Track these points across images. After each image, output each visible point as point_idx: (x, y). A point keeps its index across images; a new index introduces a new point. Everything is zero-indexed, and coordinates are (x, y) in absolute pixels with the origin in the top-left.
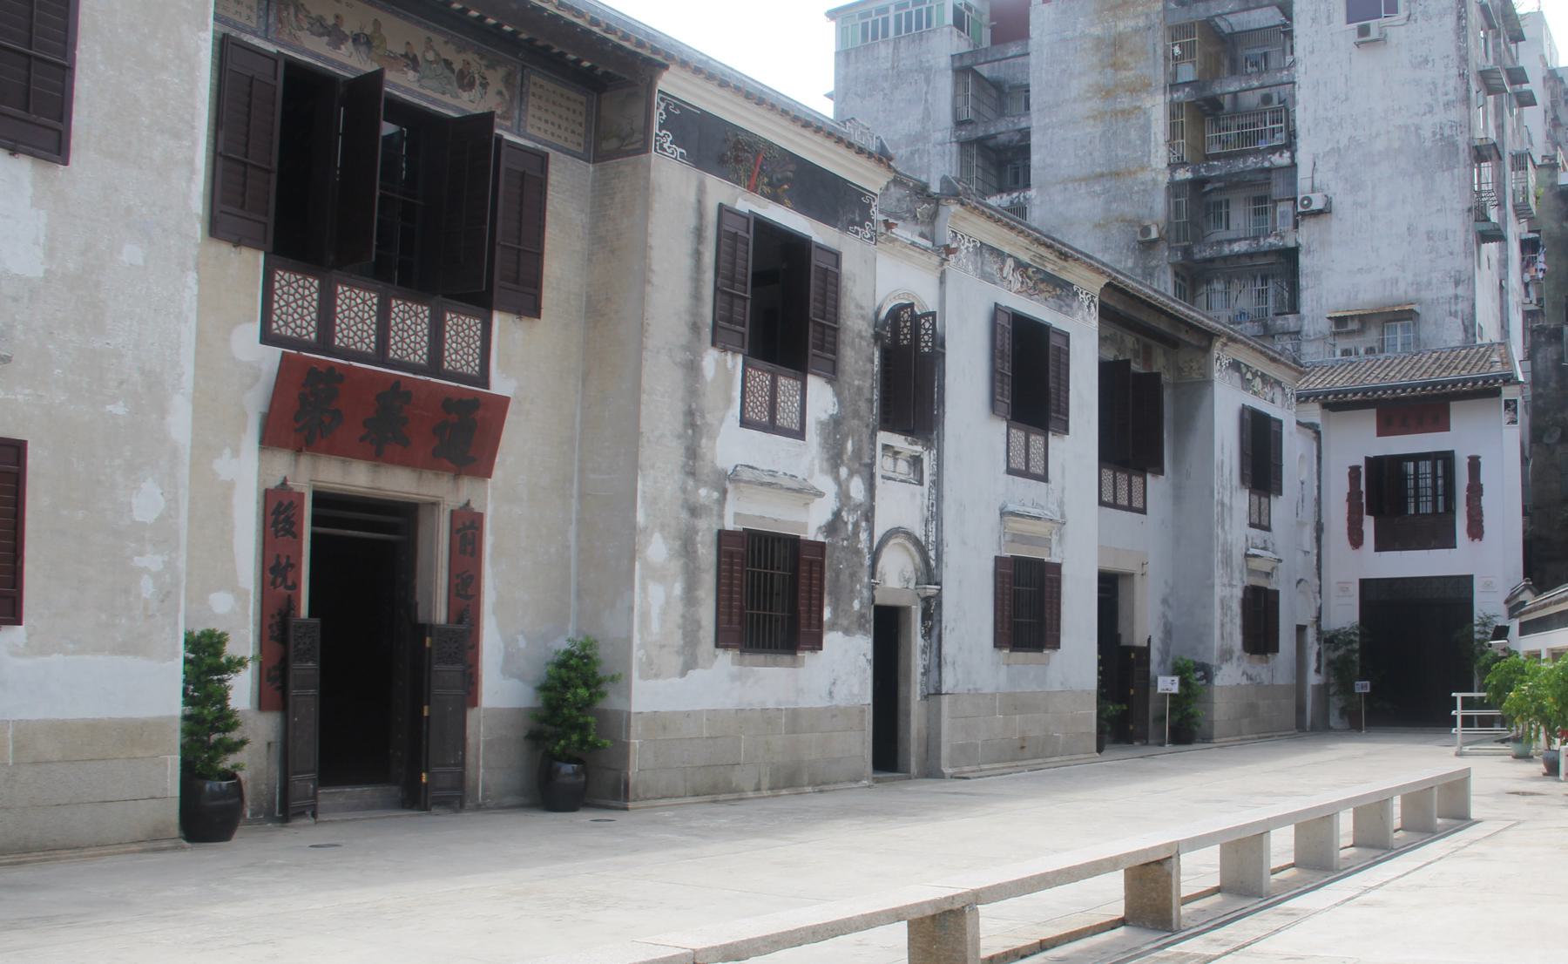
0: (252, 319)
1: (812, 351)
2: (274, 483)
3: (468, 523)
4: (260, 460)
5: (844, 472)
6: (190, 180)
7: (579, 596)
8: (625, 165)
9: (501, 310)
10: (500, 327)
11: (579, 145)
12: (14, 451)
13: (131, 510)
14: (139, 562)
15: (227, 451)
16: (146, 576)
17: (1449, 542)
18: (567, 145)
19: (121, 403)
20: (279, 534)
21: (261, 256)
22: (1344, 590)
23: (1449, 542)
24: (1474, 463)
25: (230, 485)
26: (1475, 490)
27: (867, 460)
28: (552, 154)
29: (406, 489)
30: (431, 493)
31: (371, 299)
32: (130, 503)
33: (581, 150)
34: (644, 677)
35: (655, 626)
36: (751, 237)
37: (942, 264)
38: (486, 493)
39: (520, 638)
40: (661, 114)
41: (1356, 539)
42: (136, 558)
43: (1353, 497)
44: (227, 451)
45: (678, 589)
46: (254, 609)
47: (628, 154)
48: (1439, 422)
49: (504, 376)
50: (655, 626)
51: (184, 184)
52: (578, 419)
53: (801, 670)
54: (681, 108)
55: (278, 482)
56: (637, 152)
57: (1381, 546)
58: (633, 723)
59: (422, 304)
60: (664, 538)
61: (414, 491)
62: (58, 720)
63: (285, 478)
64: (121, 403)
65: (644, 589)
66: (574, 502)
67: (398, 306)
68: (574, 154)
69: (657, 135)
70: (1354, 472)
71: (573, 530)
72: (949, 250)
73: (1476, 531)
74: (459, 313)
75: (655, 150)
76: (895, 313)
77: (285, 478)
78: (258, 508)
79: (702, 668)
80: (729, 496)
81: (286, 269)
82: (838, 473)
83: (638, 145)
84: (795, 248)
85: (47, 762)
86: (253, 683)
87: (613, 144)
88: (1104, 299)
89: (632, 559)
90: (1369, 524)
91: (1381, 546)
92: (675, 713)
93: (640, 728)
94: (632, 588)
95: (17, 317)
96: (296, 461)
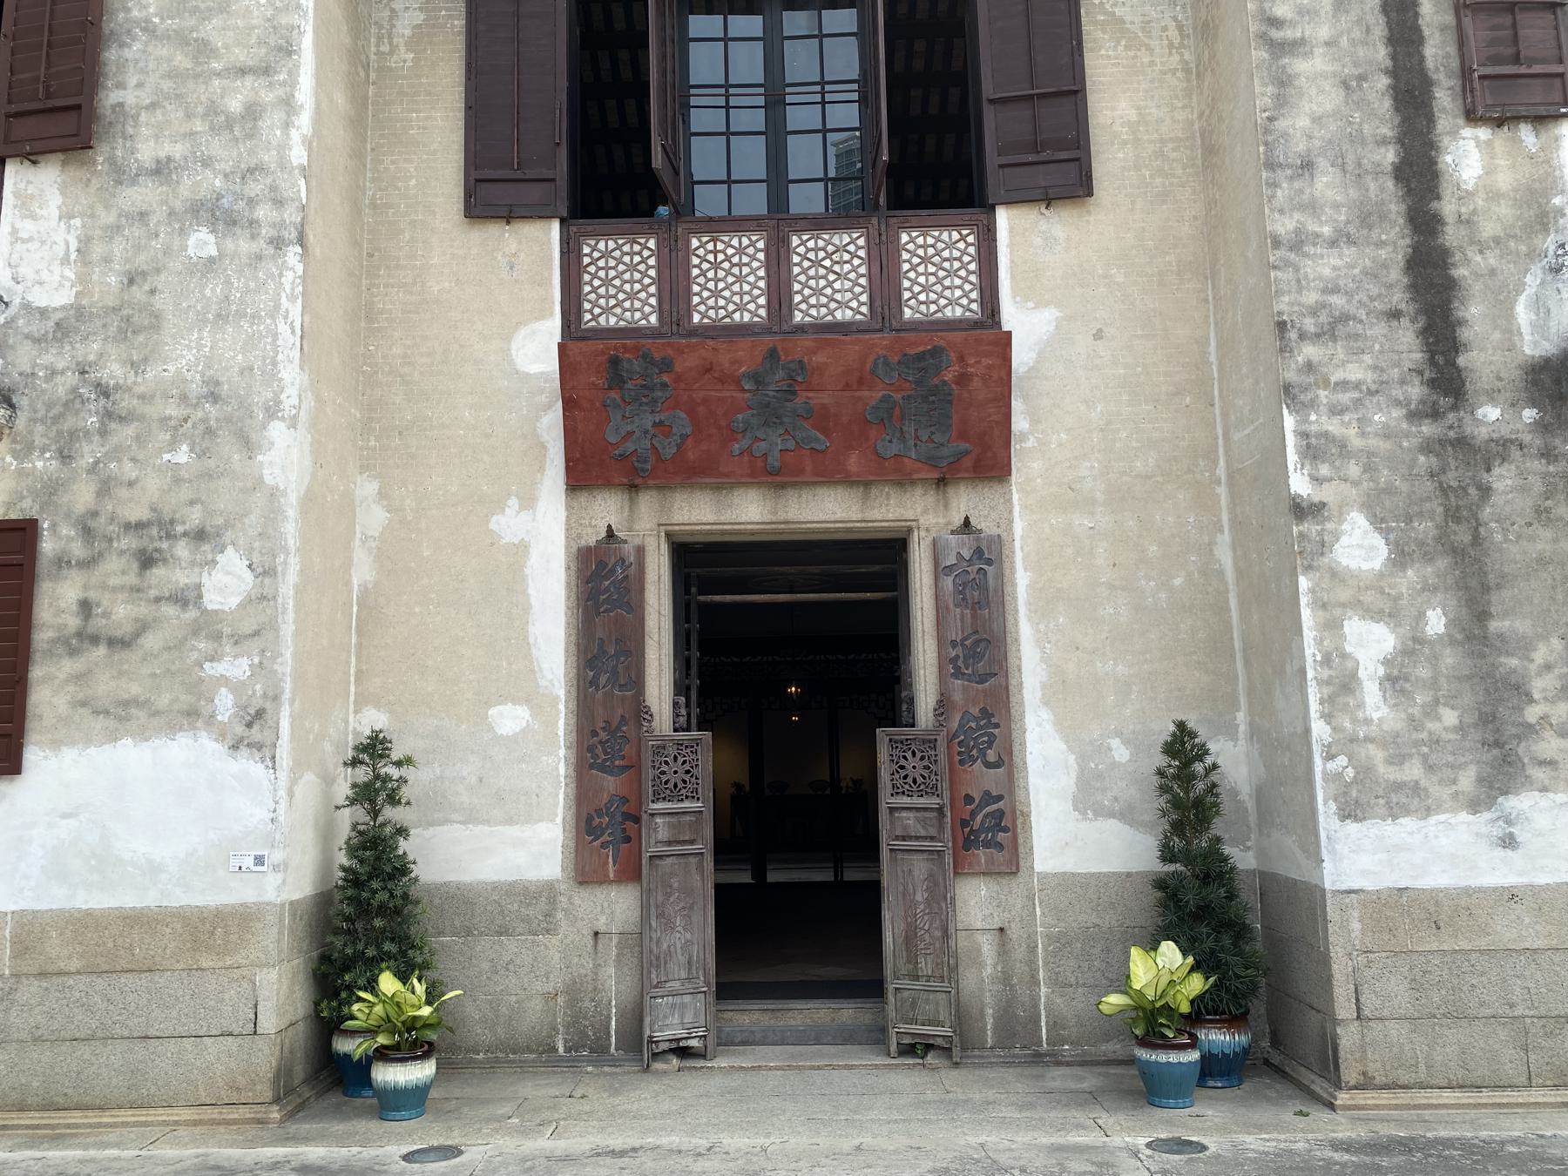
0: (543, 314)
2: (594, 535)
3: (966, 554)
4: (569, 507)
6: (287, 125)
9: (1008, 203)
10: (1011, 230)
12: (23, 533)
13: (200, 596)
14: (211, 669)
15: (513, 502)
16: (223, 690)
19: (185, 448)
20: (602, 610)
21: (555, 227)
25: (522, 549)
29: (840, 514)
30: (891, 516)
31: (753, 244)
32: (199, 586)
34: (1351, 811)
35: (1374, 703)
38: (1010, 500)
39: (1115, 743)
42: (207, 665)
44: (513, 502)
45: (1436, 623)
46: (566, 724)
49: (1031, 305)
50: (1374, 703)
51: (278, 133)
55: (603, 534)
58: (1332, 913)
59: (848, 228)
60: (1377, 522)
61: (859, 517)
62: (79, 910)
63: (609, 526)
64: (185, 448)
65: (1332, 626)
67: (803, 243)
71: (1225, 538)
74: (924, 227)
77: (609, 526)
78: (568, 576)
79: (1544, 789)
81: (598, 235)
85: (61, 973)
86: (565, 838)
92: (1468, 892)
93: (1356, 926)
95: (38, 361)
96: (632, 502)
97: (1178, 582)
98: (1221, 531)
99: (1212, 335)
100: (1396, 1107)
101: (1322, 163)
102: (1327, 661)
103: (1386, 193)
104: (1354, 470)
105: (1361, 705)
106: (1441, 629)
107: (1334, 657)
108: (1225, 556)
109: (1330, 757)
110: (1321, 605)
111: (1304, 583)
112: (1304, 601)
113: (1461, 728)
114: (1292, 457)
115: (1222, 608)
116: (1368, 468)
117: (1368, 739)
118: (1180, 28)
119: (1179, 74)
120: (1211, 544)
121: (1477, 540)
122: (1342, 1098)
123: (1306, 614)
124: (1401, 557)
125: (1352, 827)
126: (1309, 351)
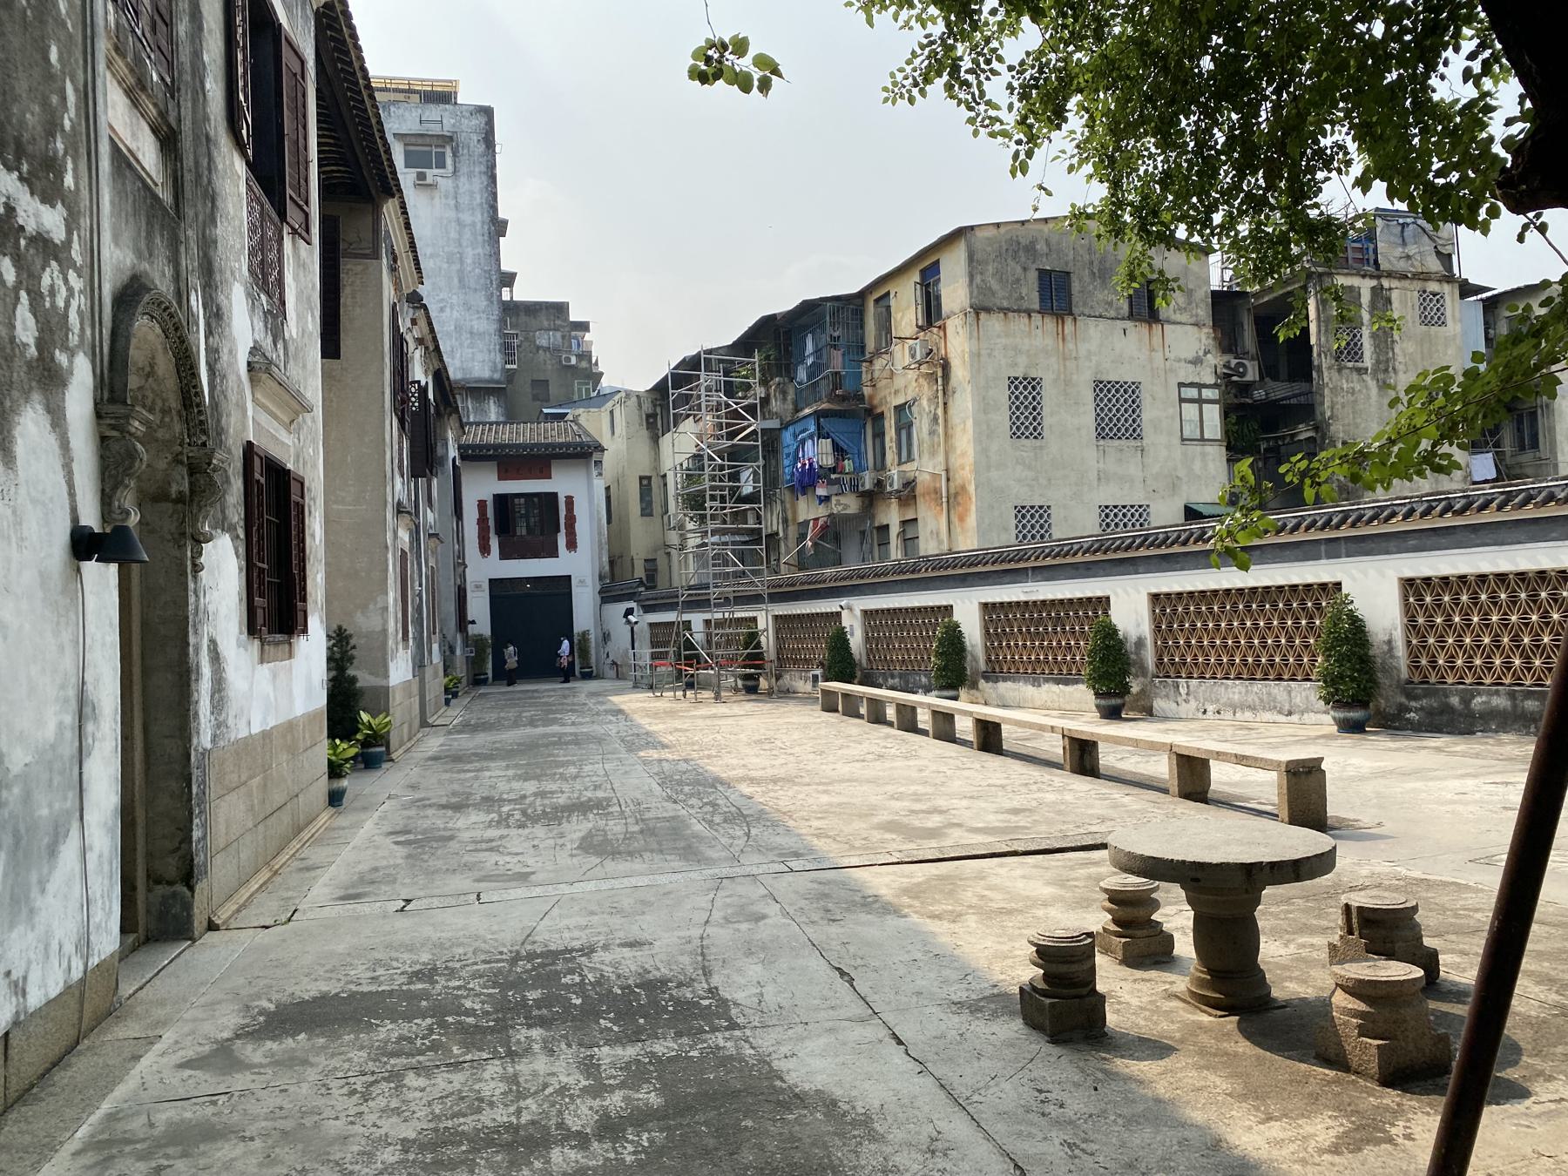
17: (553, 552)
23: (553, 552)
24: (570, 501)
41: (485, 549)
43: (482, 521)
47: (356, 256)
48: (546, 474)
56: (365, 256)
57: (504, 555)
70: (482, 505)
73: (572, 545)
83: (368, 252)
90: (494, 543)
91: (504, 555)
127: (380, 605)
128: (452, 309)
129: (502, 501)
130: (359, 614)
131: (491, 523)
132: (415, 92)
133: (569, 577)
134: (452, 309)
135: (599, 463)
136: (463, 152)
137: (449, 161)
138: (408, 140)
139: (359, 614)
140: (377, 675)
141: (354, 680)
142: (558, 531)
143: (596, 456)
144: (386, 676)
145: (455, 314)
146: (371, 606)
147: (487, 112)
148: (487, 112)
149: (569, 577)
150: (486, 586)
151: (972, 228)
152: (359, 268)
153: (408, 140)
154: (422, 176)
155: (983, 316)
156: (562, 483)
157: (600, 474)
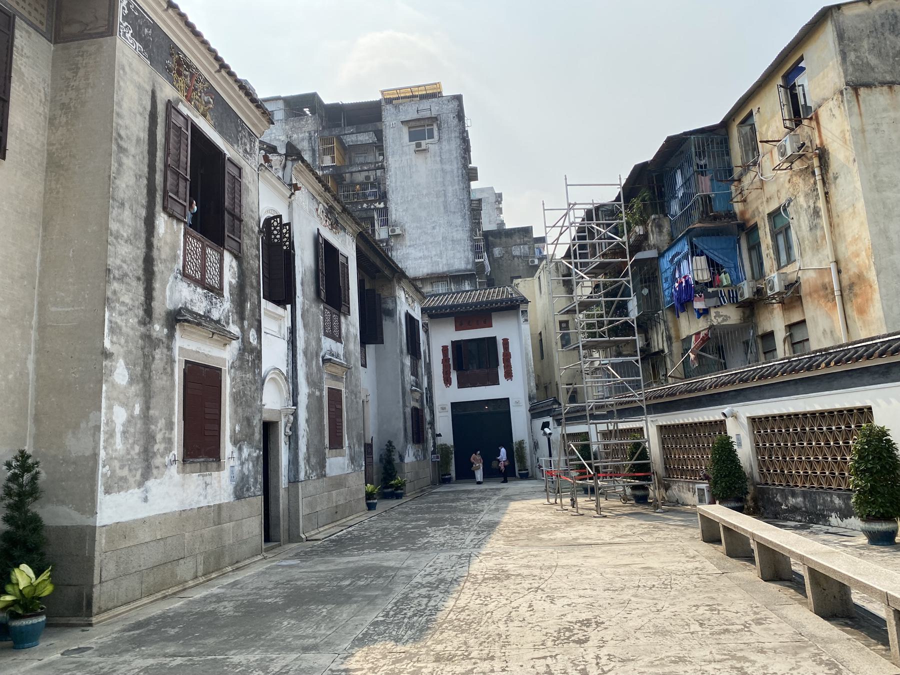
1: (226, 233)
5: (246, 323)
7: (37, 420)
8: (89, 46)
11: (41, 23)
17: (496, 382)
18: (32, 19)
22: (443, 409)
23: (496, 382)
24: (506, 342)
26: (507, 356)
27: (257, 317)
28: (17, 19)
33: (44, 28)
36: (189, 133)
37: (290, 197)
40: (123, 8)
41: (447, 381)
43: (445, 361)
47: (91, 36)
52: (38, 260)
53: (222, 472)
54: (138, 10)
56: (102, 35)
57: (461, 385)
65: (110, 408)
66: (33, 334)
68: (36, 29)
69: (121, 24)
70: (445, 349)
71: (32, 357)
72: (296, 188)
73: (509, 375)
75: (120, 35)
76: (268, 221)
80: (178, 334)
82: (242, 324)
84: (218, 154)
87: (75, 29)
88: (360, 245)
89: (100, 382)
90: (454, 376)
91: (461, 385)
94: (99, 409)
97: (10, 377)
98: (30, 353)
99: (39, 254)
100: (110, 618)
101: (127, 205)
102: (107, 424)
103: (141, 226)
104: (123, 341)
105: (115, 444)
106: (138, 413)
107: (110, 422)
108: (31, 366)
109: (104, 466)
110: (108, 398)
111: (104, 388)
112: (104, 395)
113: (139, 454)
114: (106, 331)
115: (26, 393)
116: (127, 342)
117: (116, 458)
118: (45, 94)
119: (42, 117)
120: (26, 359)
121: (150, 377)
122: (94, 620)
123: (103, 400)
124: (132, 381)
125: (108, 497)
126: (115, 285)
127: (91, 424)
128: (440, 226)
129: (456, 345)
130: (70, 435)
131: (451, 362)
132: (416, 96)
133: (508, 399)
134: (440, 226)
135: (525, 312)
136: (444, 126)
137: (436, 133)
138: (411, 124)
139: (70, 435)
140: (83, 512)
141: (36, 520)
142: (498, 365)
143: (522, 307)
144: (94, 513)
145: (442, 230)
146: (83, 425)
147: (458, 98)
148: (458, 98)
149: (508, 399)
150: (449, 408)
151: (839, 7)
152: (92, 49)
153: (411, 124)
154: (418, 145)
155: (862, 91)
156: (499, 329)
157: (526, 320)
